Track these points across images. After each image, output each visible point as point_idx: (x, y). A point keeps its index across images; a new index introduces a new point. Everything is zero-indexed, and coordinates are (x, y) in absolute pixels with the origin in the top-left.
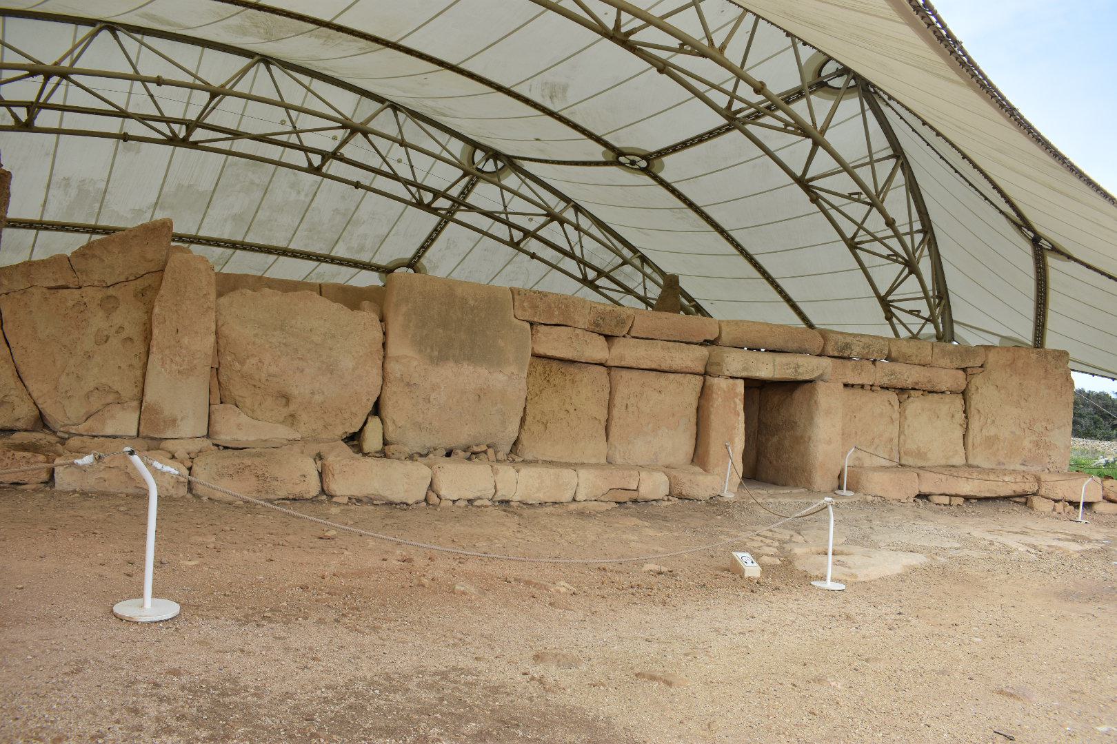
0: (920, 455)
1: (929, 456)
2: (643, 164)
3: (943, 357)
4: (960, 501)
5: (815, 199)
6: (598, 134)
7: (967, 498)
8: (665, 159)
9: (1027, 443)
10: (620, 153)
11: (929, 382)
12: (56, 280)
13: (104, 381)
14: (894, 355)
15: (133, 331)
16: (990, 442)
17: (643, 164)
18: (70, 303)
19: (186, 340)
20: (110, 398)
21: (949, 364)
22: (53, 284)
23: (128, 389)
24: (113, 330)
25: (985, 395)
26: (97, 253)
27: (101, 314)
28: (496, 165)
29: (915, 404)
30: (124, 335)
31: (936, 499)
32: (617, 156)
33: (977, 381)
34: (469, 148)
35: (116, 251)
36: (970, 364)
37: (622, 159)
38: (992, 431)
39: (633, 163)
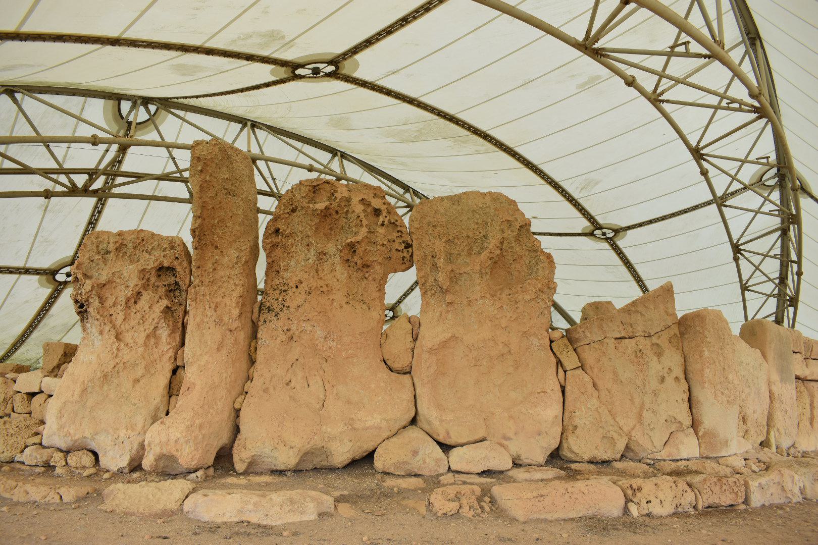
2: (610, 234)
5: (736, 259)
6: (593, 213)
8: (629, 232)
10: (600, 227)
12: (620, 332)
13: (671, 413)
15: (678, 372)
17: (610, 234)
18: (630, 351)
19: (730, 377)
20: (674, 427)
22: (619, 336)
23: (687, 421)
24: (666, 370)
26: (640, 309)
27: (655, 358)
30: (674, 375)
32: (595, 229)
35: (652, 307)
37: (597, 232)
39: (604, 234)
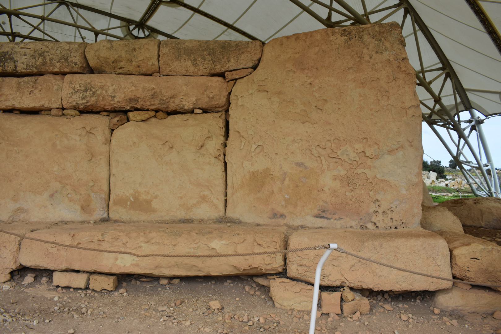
0: (139, 204)
1: (155, 204)
3: (178, 58)
4: (108, 283)
7: (123, 279)
9: (328, 181)
11: (154, 96)
14: (92, 63)
16: (258, 181)
21: (192, 69)
25: (249, 104)
28: (144, 32)
29: (127, 132)
31: (59, 279)
33: (238, 88)
34: (124, 23)
36: (232, 65)
38: (260, 164)
